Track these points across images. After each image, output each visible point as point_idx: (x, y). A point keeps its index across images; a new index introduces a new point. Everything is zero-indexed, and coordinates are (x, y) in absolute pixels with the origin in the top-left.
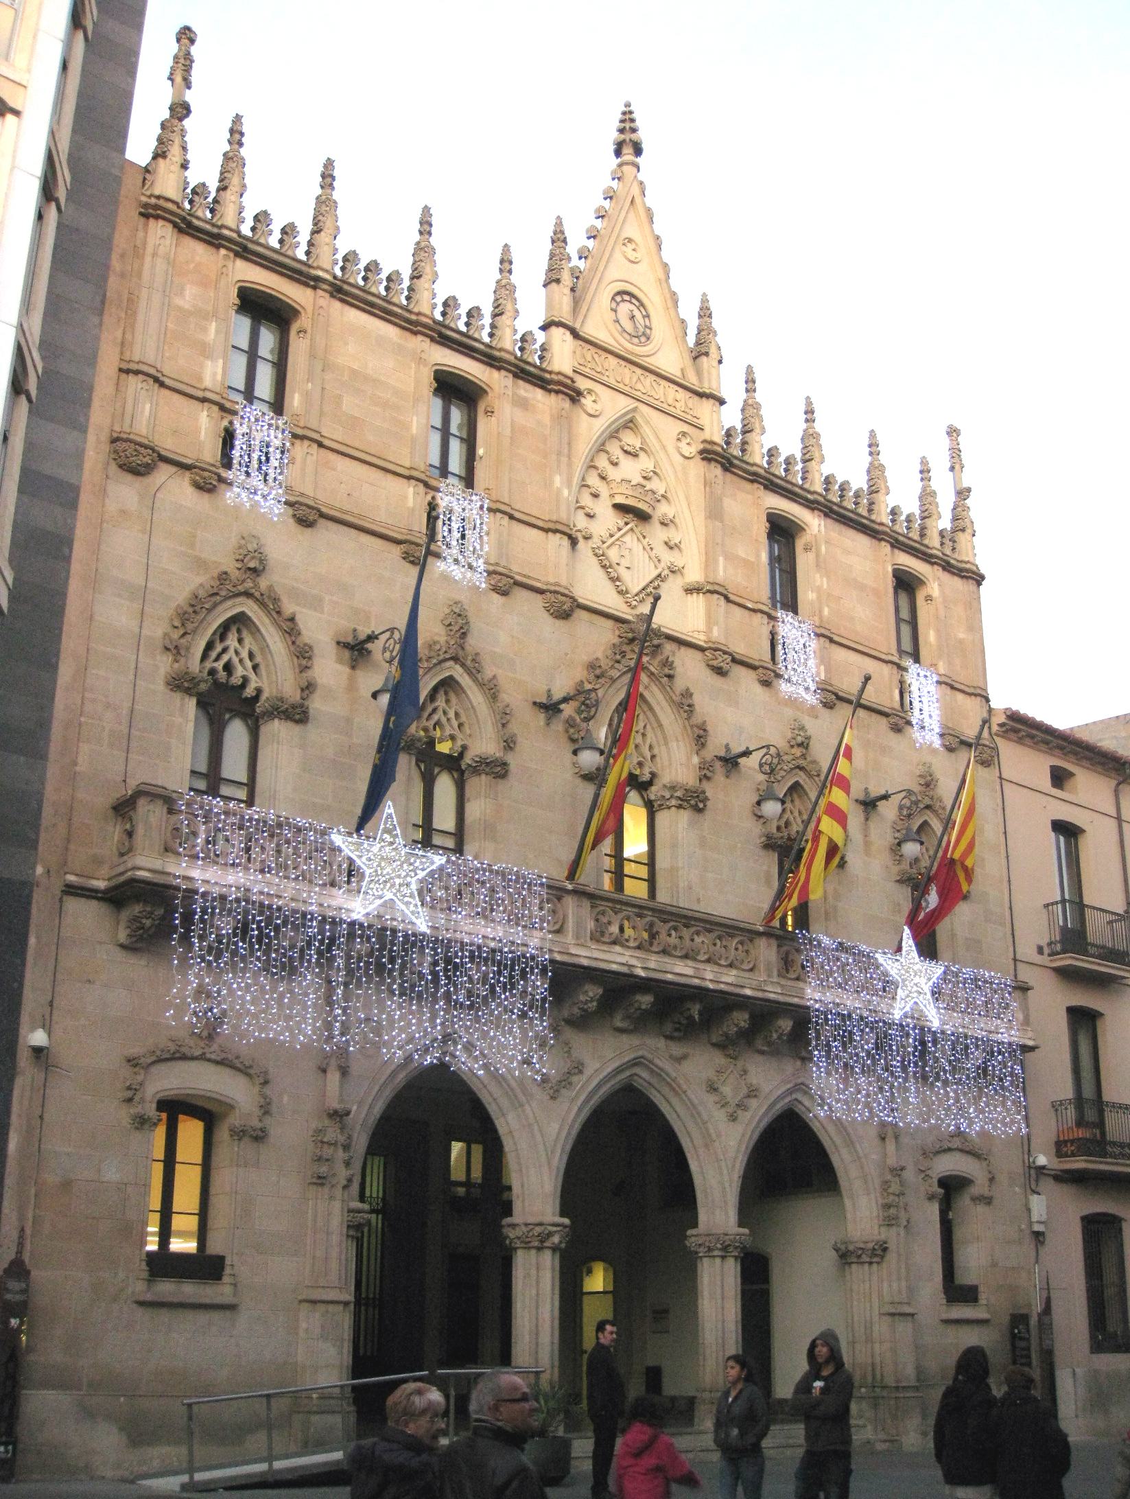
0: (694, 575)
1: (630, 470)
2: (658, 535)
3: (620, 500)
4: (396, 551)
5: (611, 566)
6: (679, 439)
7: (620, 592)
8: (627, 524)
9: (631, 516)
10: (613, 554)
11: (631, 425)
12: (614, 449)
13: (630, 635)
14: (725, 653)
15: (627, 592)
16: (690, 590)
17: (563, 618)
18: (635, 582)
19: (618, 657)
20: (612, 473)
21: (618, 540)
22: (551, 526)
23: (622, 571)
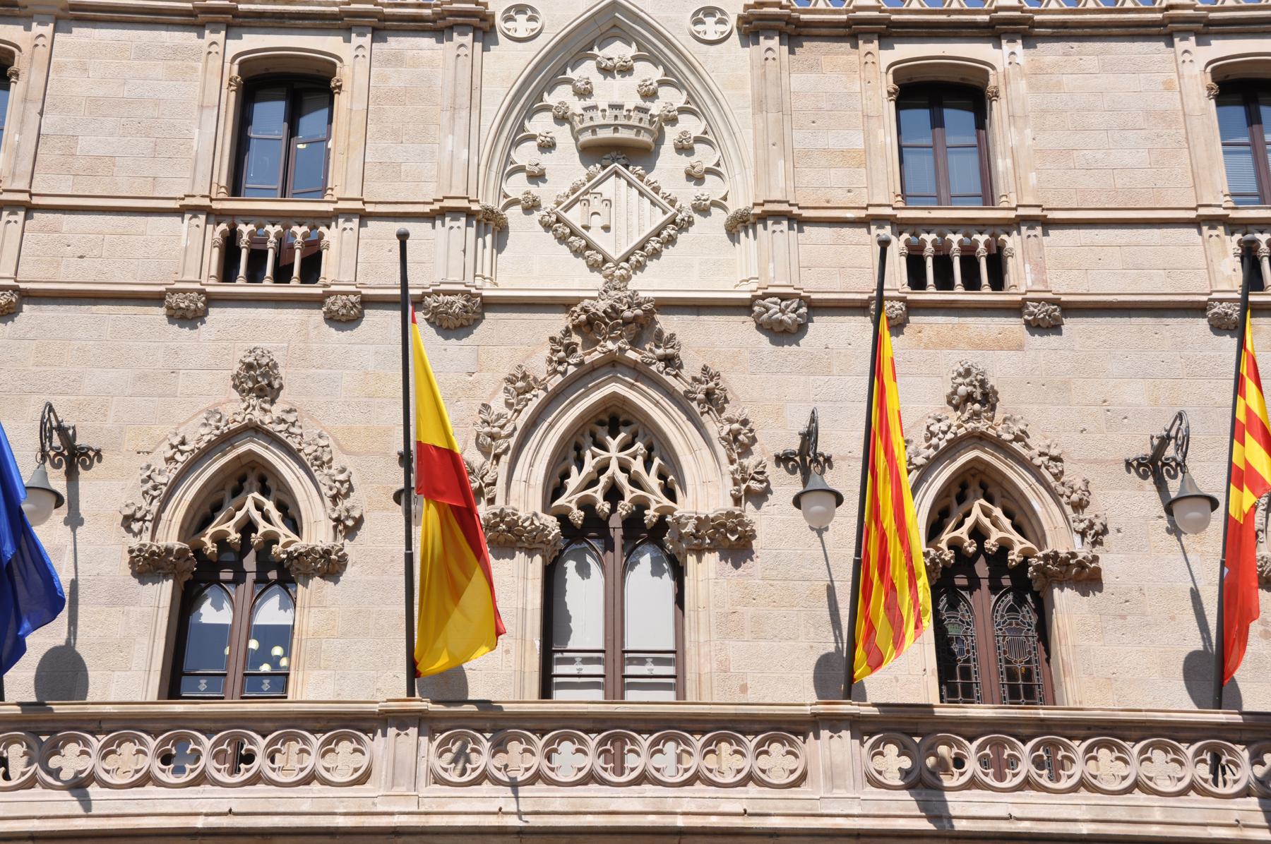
0: (739, 203)
1: (623, 91)
2: (668, 166)
3: (586, 137)
4: (159, 313)
5: (572, 233)
6: (698, 22)
7: (594, 267)
8: (604, 167)
9: (614, 154)
10: (575, 216)
11: (615, 31)
12: (586, 71)
13: (583, 317)
14: (784, 297)
15: (605, 261)
16: (741, 225)
17: (462, 326)
18: (614, 246)
19: (562, 354)
20: (576, 105)
21: (586, 192)
22: (437, 206)
23: (596, 236)
